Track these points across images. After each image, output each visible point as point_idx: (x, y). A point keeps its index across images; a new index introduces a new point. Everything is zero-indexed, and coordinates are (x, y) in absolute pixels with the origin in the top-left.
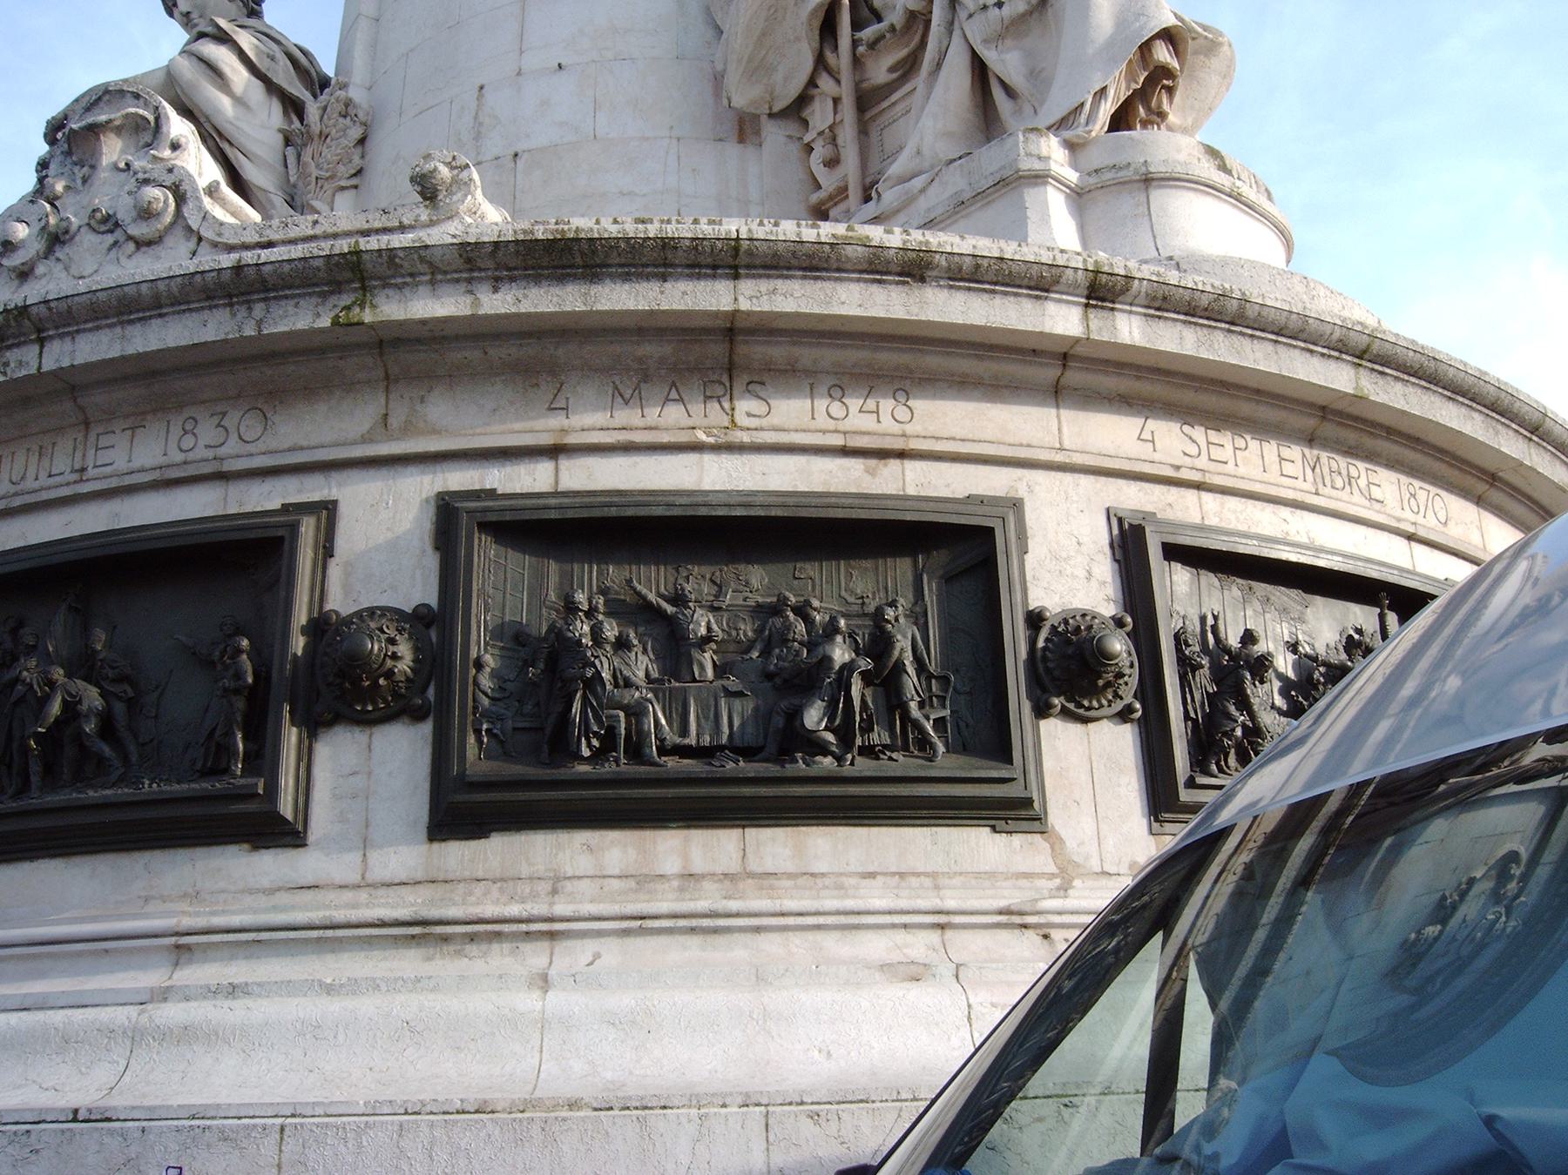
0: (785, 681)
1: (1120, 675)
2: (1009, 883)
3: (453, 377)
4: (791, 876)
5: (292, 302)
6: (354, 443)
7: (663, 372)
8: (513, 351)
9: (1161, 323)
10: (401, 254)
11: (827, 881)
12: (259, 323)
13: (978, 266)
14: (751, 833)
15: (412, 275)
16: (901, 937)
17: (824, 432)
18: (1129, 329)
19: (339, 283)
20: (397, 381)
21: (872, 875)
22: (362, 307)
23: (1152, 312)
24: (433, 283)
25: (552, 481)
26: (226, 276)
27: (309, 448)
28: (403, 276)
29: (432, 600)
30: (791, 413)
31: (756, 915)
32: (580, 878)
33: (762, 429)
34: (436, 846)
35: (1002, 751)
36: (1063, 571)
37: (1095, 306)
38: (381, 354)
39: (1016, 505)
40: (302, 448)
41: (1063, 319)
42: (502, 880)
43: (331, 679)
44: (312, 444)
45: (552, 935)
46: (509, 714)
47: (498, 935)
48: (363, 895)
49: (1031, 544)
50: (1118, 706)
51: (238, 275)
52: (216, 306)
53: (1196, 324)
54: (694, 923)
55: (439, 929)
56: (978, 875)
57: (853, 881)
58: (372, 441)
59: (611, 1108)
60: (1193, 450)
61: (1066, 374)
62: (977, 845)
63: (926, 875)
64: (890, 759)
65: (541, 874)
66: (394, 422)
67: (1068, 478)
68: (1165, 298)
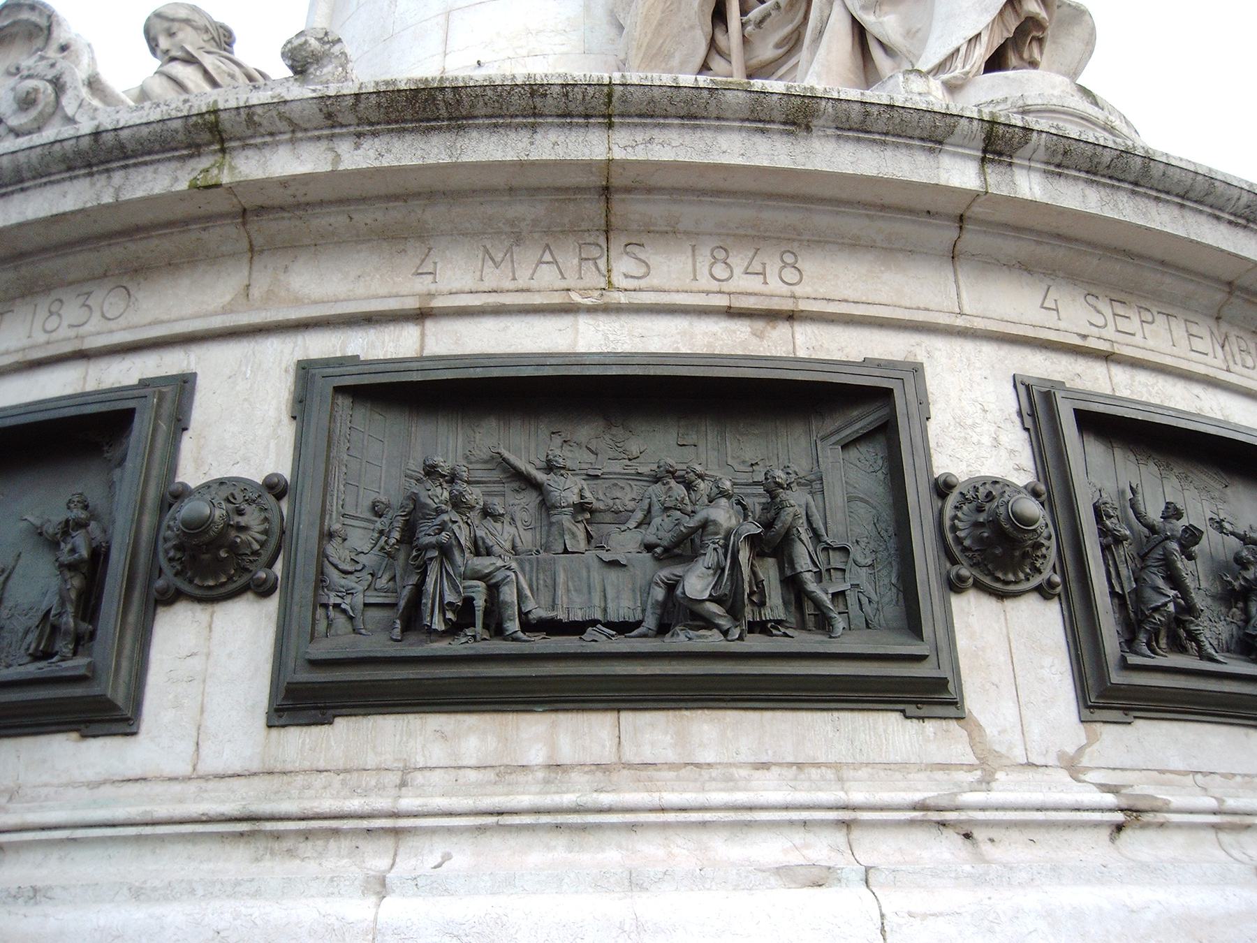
0: (666, 550)
1: (1039, 546)
2: (922, 776)
3: (318, 245)
4: (672, 766)
5: (151, 168)
6: (215, 314)
7: (536, 236)
8: (379, 215)
9: (1062, 181)
10: (259, 111)
11: (714, 773)
12: (118, 190)
13: (867, 114)
14: (627, 718)
15: (272, 134)
16: (799, 837)
17: (708, 293)
18: (1028, 185)
19: (198, 146)
20: (262, 251)
21: (765, 766)
22: (220, 168)
23: (1052, 168)
24: (292, 141)
25: (417, 346)
26: (85, 143)
27: (168, 321)
28: (263, 136)
29: (285, 471)
30: (672, 271)
32: (431, 769)
33: (640, 290)
34: (274, 732)
35: (913, 625)
36: (972, 433)
37: (992, 161)
38: (244, 224)
39: (916, 370)
40: (162, 322)
41: (959, 173)
42: (346, 771)
43: (172, 554)
44: (173, 317)
46: (360, 588)
47: (336, 832)
48: (192, 787)
49: (933, 411)
50: (1036, 581)
51: (96, 141)
52: (76, 177)
53: (1098, 183)
54: (560, 819)
55: (269, 826)
56: (888, 766)
57: (744, 772)
58: (232, 311)
61: (961, 233)
63: (827, 765)
64: (786, 635)
65: (388, 764)
66: (256, 292)
67: (969, 346)
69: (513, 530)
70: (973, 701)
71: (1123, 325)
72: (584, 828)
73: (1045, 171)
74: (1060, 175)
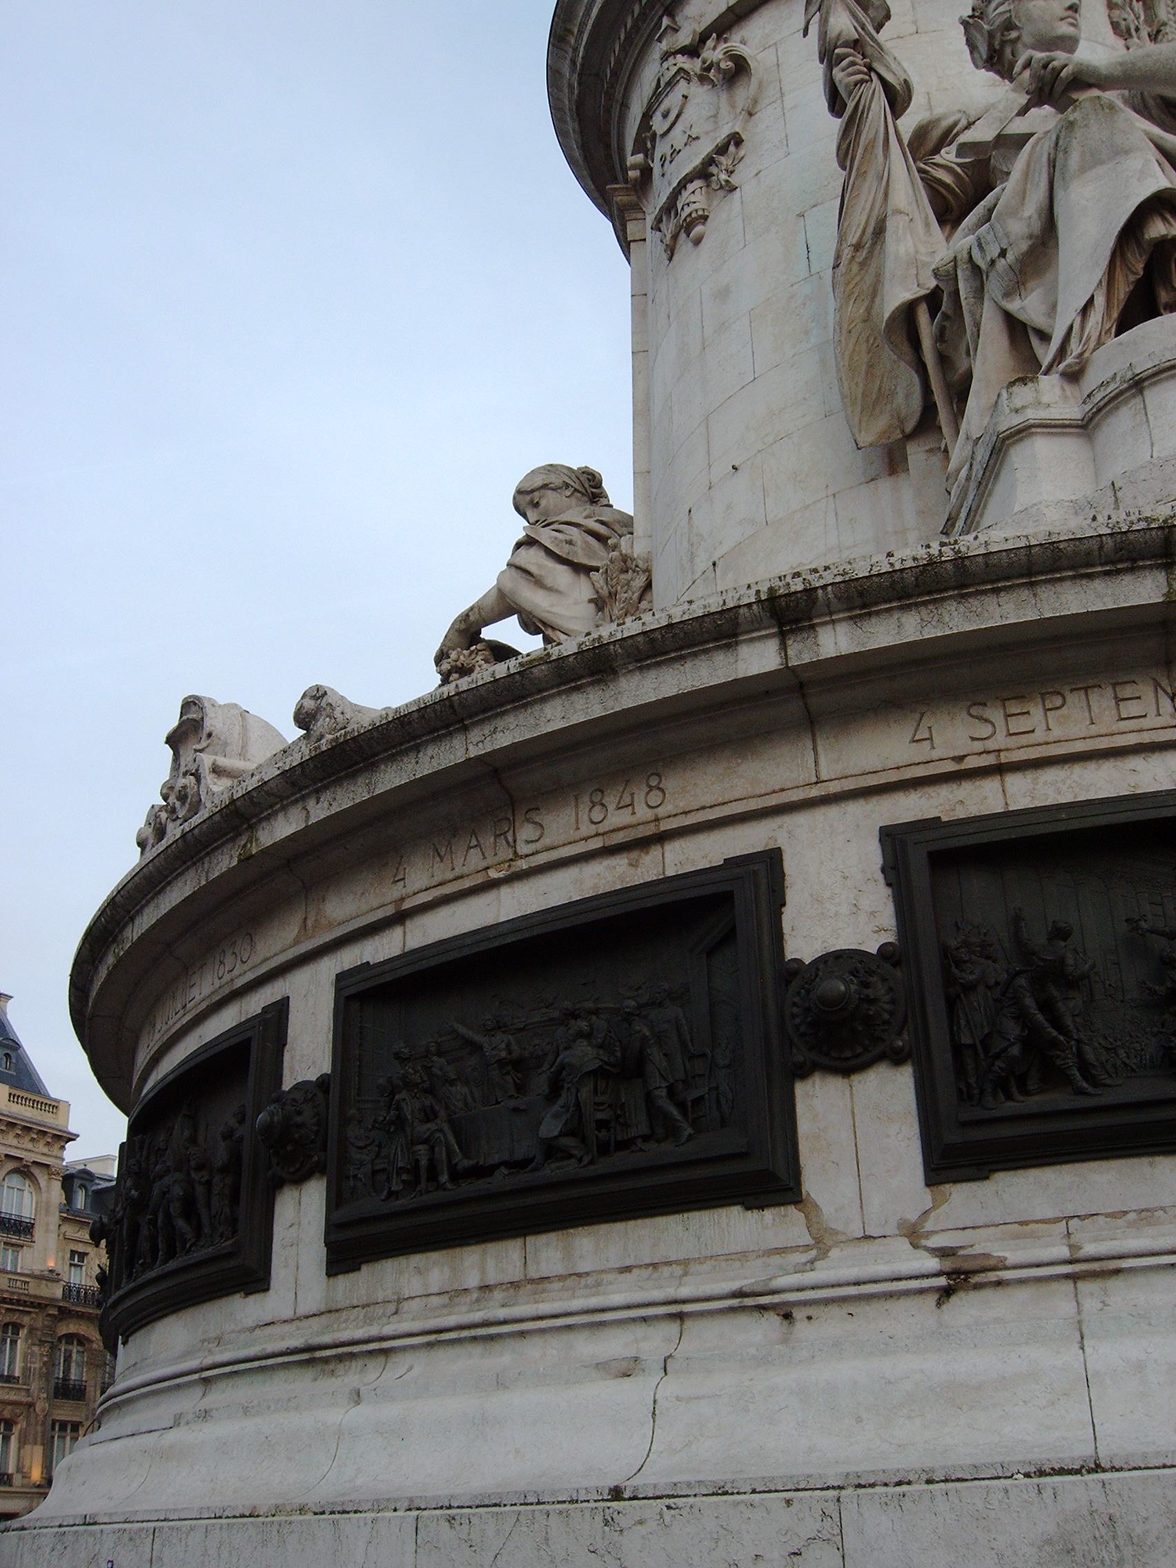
2: (759, 1262)
4: (561, 1278)
11: (590, 1280)
13: (652, 641)
14: (531, 1240)
16: (640, 1330)
17: (586, 839)
18: (835, 641)
21: (628, 1269)
30: (563, 826)
31: (521, 1320)
32: (413, 1298)
34: (332, 1279)
37: (792, 631)
41: (759, 658)
42: (368, 1305)
45: (386, 1352)
47: (352, 1356)
54: (473, 1332)
56: (729, 1257)
57: (611, 1277)
59: (323, 1513)
60: (985, 730)
62: (735, 1227)
63: (677, 1262)
67: (833, 811)
68: (861, 594)
69: (465, 1090)
70: (811, 1184)
71: (1017, 725)
72: (491, 1338)
73: (851, 618)
74: (870, 614)
